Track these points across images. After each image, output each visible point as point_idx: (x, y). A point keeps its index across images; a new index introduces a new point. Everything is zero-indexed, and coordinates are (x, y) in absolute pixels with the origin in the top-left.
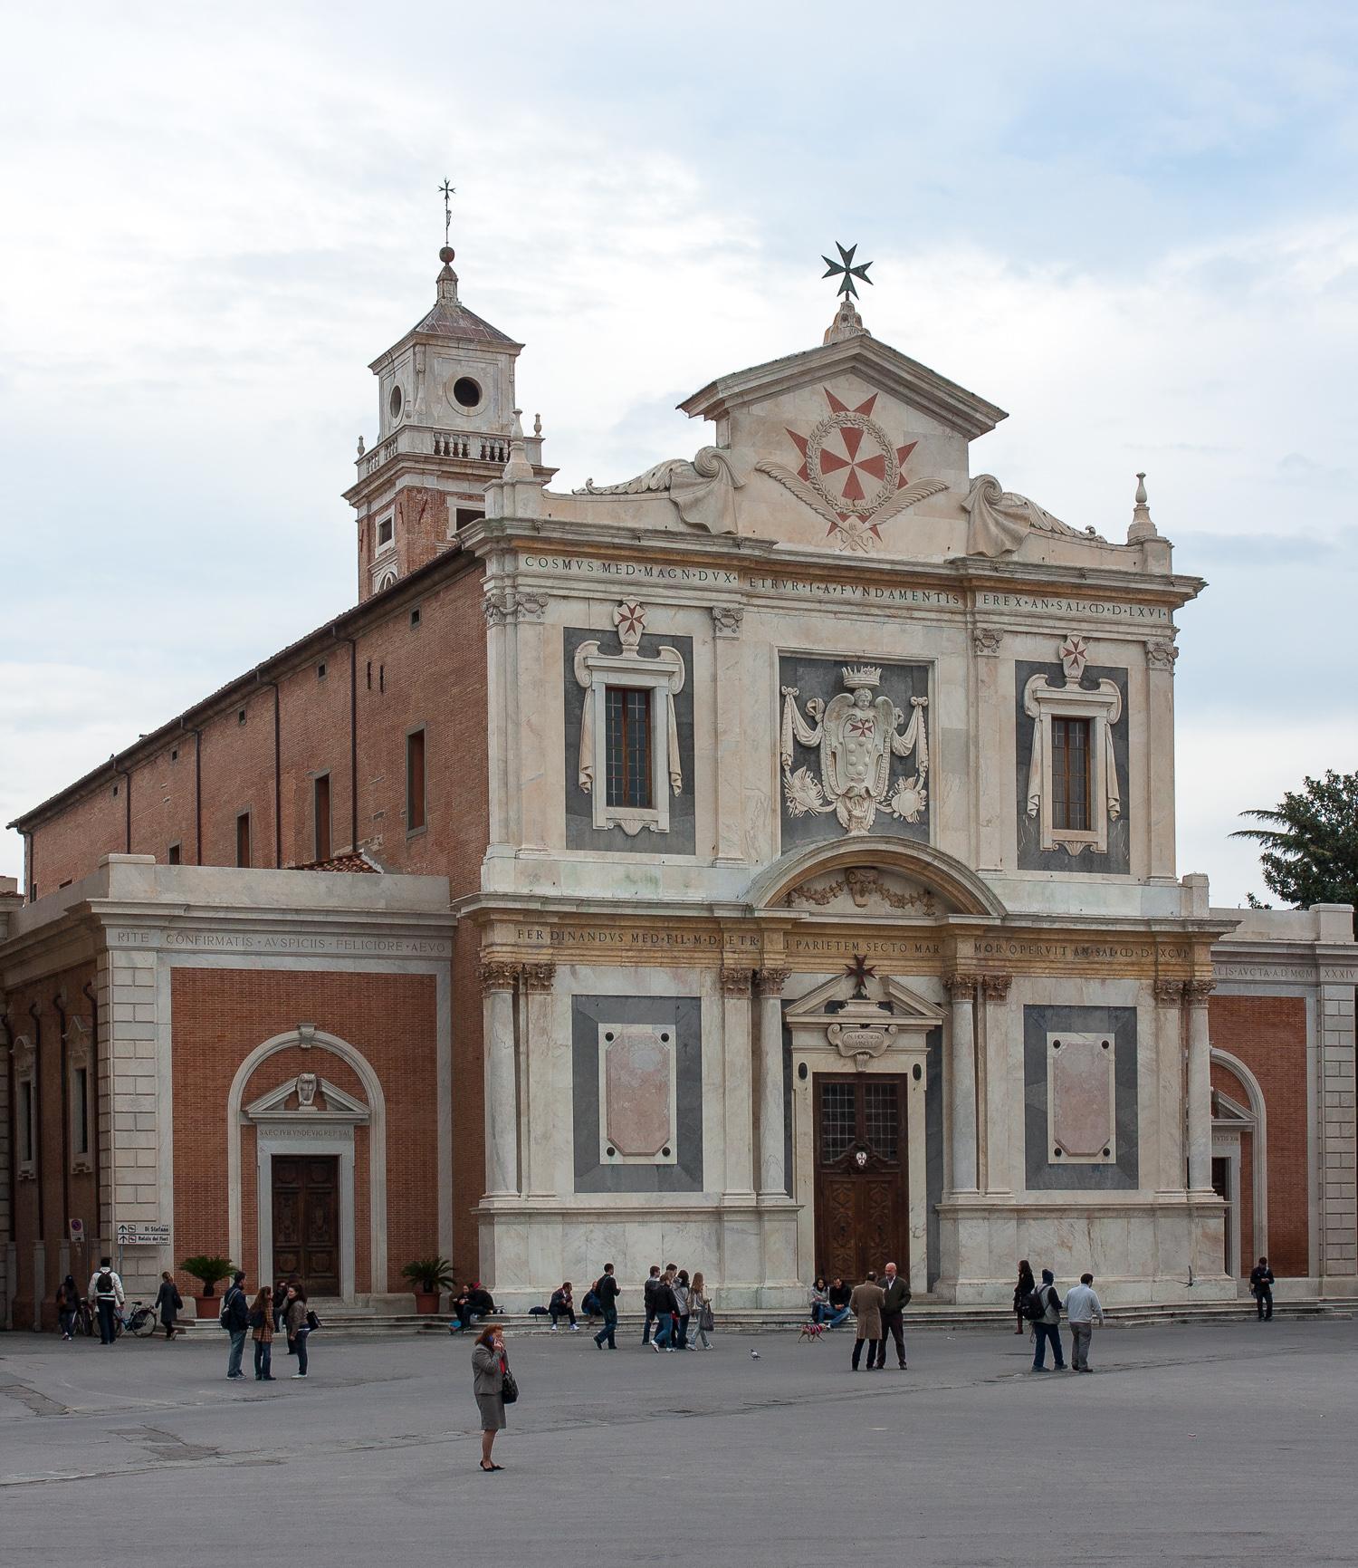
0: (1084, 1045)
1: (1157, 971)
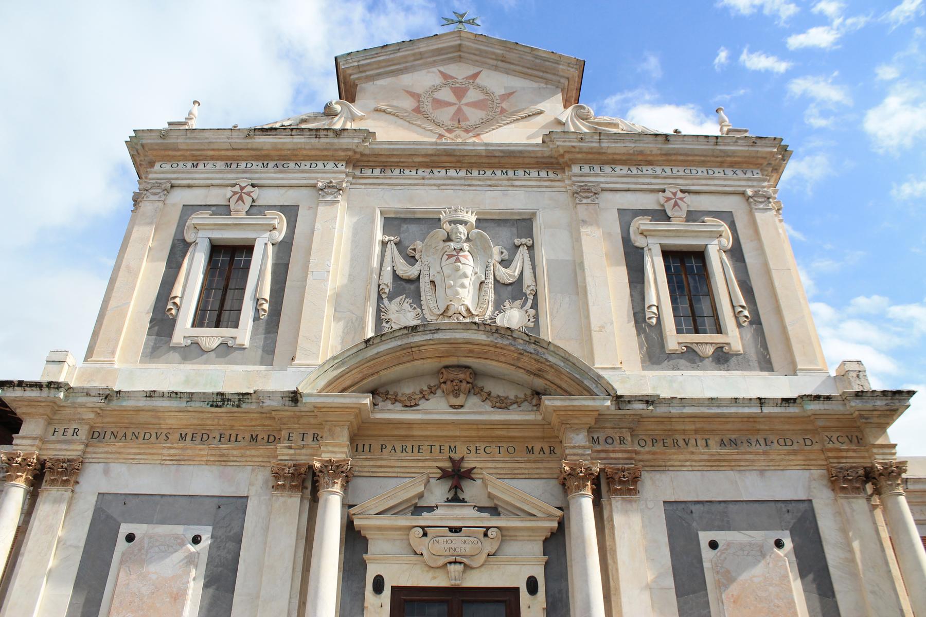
0: (750, 544)
1: (827, 459)
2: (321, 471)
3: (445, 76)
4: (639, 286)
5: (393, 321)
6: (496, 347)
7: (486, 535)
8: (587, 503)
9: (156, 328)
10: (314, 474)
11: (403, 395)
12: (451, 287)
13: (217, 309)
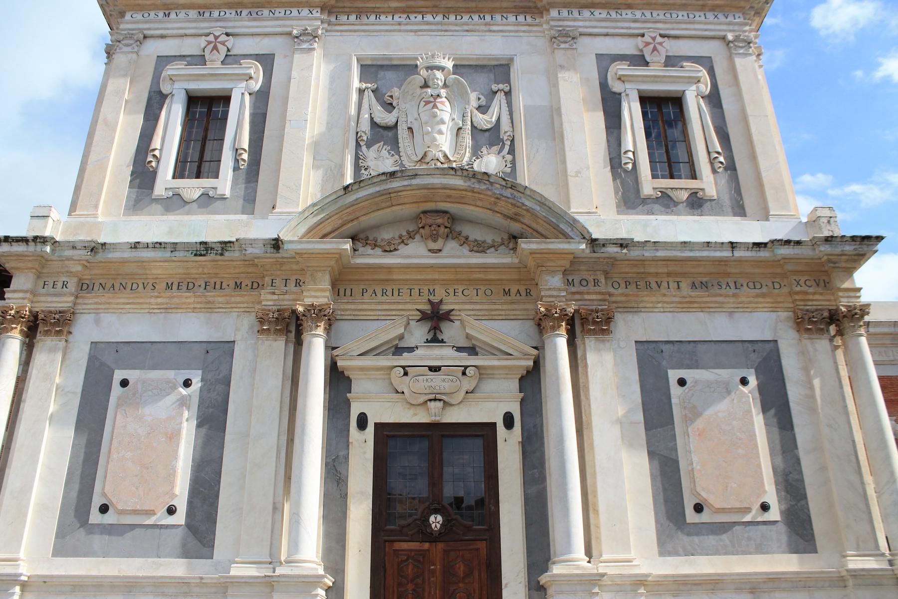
2: (304, 315)
4: (616, 131)
5: (372, 168)
6: (473, 192)
7: (464, 373)
8: (562, 343)
9: (138, 181)
10: (298, 318)
11: (382, 240)
12: (428, 133)
13: (197, 160)
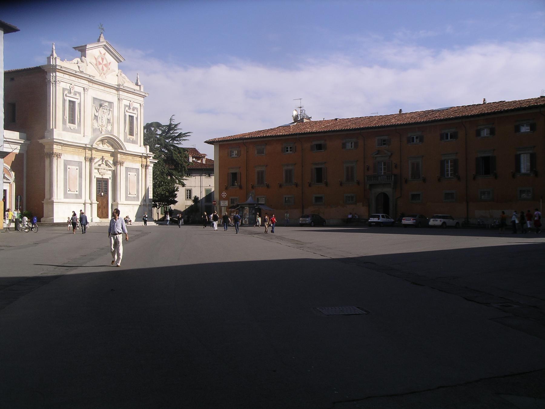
3: (101, 53)
